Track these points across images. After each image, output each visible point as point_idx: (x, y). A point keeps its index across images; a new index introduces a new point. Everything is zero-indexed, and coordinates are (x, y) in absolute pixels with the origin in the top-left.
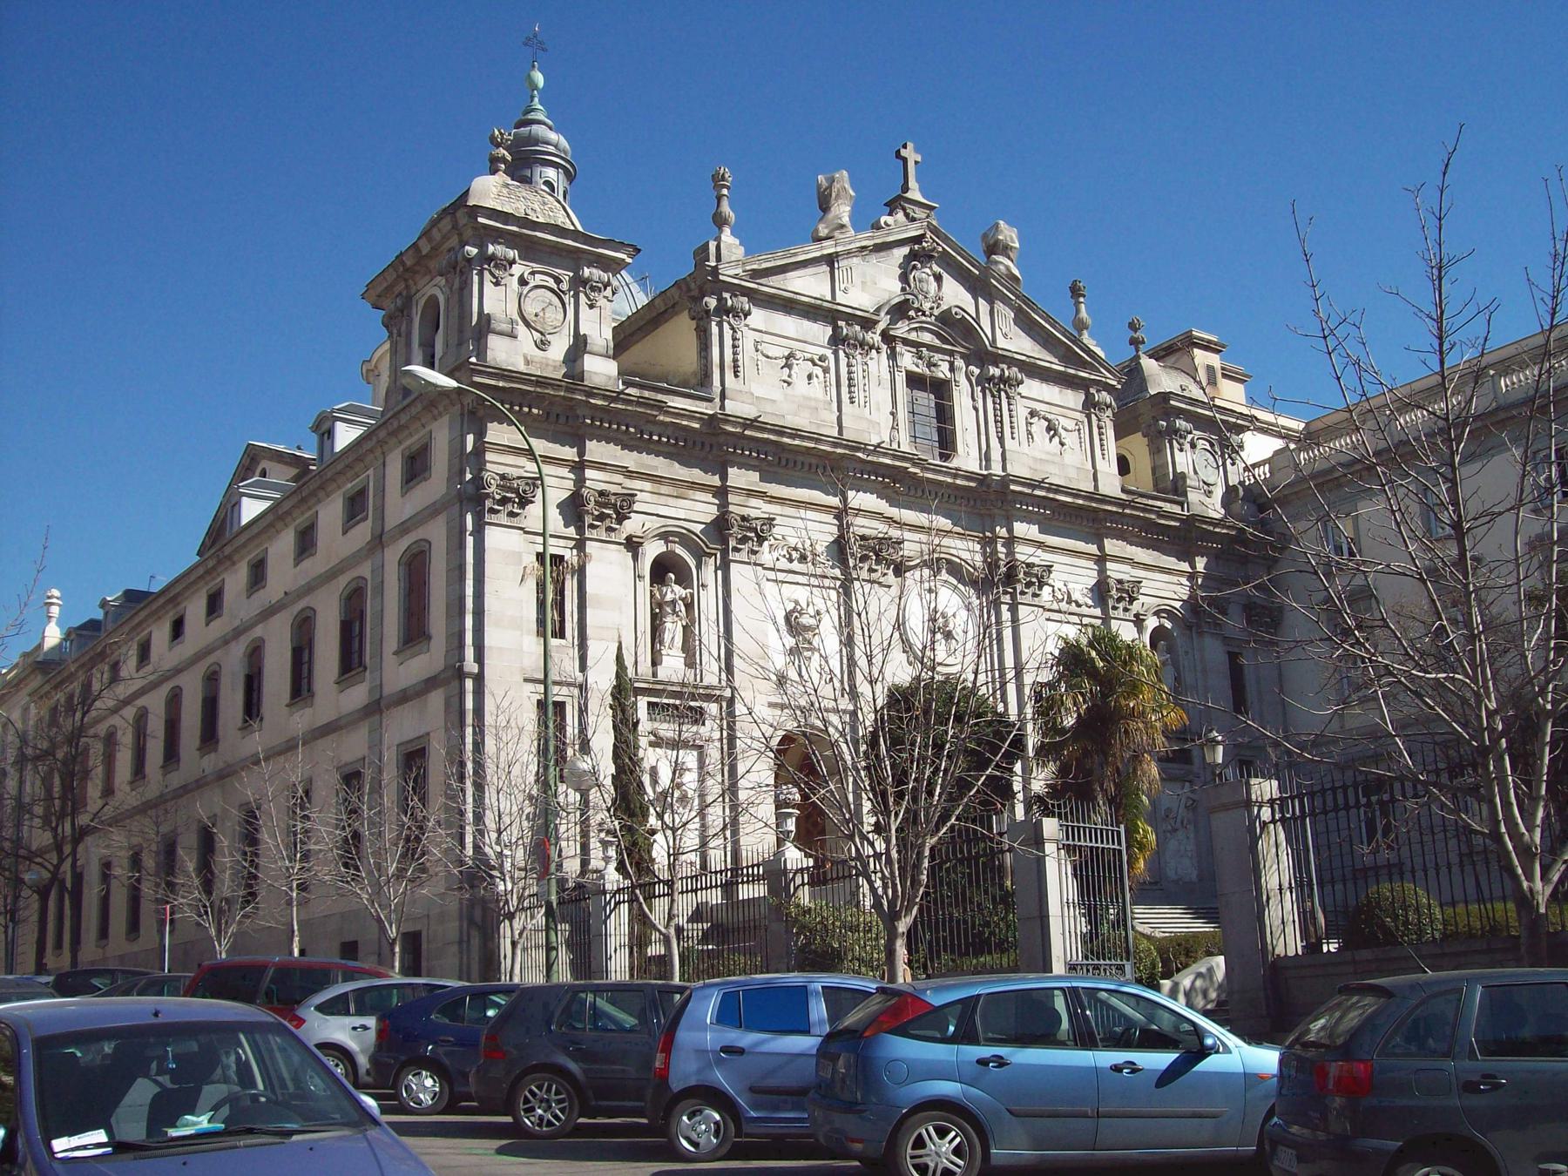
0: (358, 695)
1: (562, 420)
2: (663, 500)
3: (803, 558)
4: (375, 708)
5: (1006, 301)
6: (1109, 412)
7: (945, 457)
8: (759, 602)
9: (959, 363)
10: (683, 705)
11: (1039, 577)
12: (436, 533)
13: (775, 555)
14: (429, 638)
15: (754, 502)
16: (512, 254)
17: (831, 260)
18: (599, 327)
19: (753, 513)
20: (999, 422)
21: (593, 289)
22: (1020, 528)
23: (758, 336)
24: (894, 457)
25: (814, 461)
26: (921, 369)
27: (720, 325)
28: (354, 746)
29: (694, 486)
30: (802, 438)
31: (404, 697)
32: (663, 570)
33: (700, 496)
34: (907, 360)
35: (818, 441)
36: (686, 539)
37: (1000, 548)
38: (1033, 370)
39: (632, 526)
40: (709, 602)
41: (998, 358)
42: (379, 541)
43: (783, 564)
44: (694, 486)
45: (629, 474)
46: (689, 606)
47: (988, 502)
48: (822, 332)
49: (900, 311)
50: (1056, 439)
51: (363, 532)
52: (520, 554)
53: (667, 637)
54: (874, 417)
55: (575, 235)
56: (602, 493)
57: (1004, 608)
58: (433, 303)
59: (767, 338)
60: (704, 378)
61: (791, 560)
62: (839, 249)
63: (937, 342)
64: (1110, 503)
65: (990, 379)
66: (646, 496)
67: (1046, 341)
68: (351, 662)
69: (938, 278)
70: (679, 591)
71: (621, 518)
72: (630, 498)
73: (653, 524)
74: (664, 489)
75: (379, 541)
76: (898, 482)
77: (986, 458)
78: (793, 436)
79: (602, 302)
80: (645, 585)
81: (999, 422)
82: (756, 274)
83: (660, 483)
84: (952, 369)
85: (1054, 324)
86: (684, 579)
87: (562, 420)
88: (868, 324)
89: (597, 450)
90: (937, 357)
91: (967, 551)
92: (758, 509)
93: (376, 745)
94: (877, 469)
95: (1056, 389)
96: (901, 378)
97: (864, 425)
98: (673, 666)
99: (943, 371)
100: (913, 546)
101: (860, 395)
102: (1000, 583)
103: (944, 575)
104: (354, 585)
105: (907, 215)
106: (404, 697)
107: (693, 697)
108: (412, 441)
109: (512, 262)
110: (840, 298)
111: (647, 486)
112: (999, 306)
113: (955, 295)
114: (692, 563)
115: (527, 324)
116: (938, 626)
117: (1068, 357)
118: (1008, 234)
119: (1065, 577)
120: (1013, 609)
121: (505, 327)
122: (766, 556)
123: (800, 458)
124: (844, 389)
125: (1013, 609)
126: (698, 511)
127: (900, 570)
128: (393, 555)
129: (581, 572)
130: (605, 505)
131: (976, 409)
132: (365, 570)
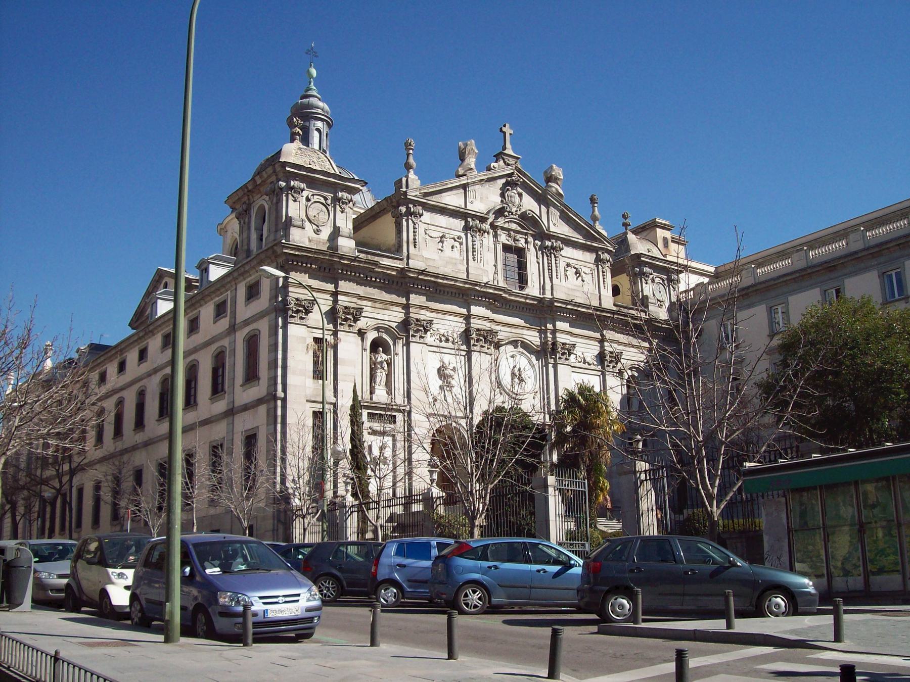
0: (221, 406)
1: (327, 270)
2: (377, 310)
3: (447, 340)
4: (231, 413)
5: (555, 207)
6: (608, 264)
7: (522, 288)
9: (530, 239)
10: (385, 414)
11: (569, 350)
12: (263, 326)
13: (433, 338)
14: (259, 379)
15: (423, 312)
16: (303, 185)
17: (464, 187)
18: (345, 223)
19: (422, 318)
20: (550, 270)
21: (343, 203)
22: (560, 325)
23: (426, 226)
24: (495, 289)
25: (454, 291)
27: (407, 221)
28: (219, 431)
29: (393, 303)
30: (447, 279)
31: (246, 408)
32: (376, 345)
34: (503, 238)
35: (456, 281)
36: (387, 330)
37: (549, 335)
39: (361, 324)
40: (399, 363)
41: (550, 237)
42: (233, 329)
43: (437, 343)
44: (393, 303)
45: (360, 297)
46: (389, 364)
47: (542, 312)
48: (459, 224)
49: (500, 213)
51: (224, 323)
52: (305, 339)
53: (378, 379)
55: (334, 176)
56: (346, 308)
57: (550, 366)
58: (262, 208)
60: (398, 248)
61: (441, 341)
63: (519, 229)
65: (546, 247)
66: (368, 310)
68: (217, 389)
69: (520, 195)
70: (385, 357)
71: (356, 320)
72: (360, 310)
73: (371, 323)
74: (378, 305)
75: (233, 329)
76: (497, 301)
77: (543, 288)
78: (443, 279)
79: (347, 209)
80: (367, 354)
81: (550, 270)
84: (526, 242)
86: (387, 351)
87: (327, 270)
88: (483, 220)
89: (344, 286)
90: (518, 236)
91: (533, 337)
92: (424, 315)
93: (231, 431)
94: (486, 295)
95: (581, 252)
96: (500, 247)
97: (480, 272)
98: (381, 395)
99: (522, 243)
100: (504, 334)
102: (548, 352)
104: (219, 350)
105: (505, 162)
106: (246, 408)
107: (389, 410)
108: (251, 279)
110: (469, 207)
111: (369, 303)
112: (552, 209)
113: (529, 204)
114: (391, 342)
115: (310, 221)
116: (517, 375)
117: (588, 235)
118: (558, 172)
119: (583, 350)
121: (299, 223)
124: (470, 254)
126: (395, 316)
127: (498, 346)
128: (241, 336)
129: (335, 347)
130: (348, 314)
131: (538, 263)
132: (225, 342)
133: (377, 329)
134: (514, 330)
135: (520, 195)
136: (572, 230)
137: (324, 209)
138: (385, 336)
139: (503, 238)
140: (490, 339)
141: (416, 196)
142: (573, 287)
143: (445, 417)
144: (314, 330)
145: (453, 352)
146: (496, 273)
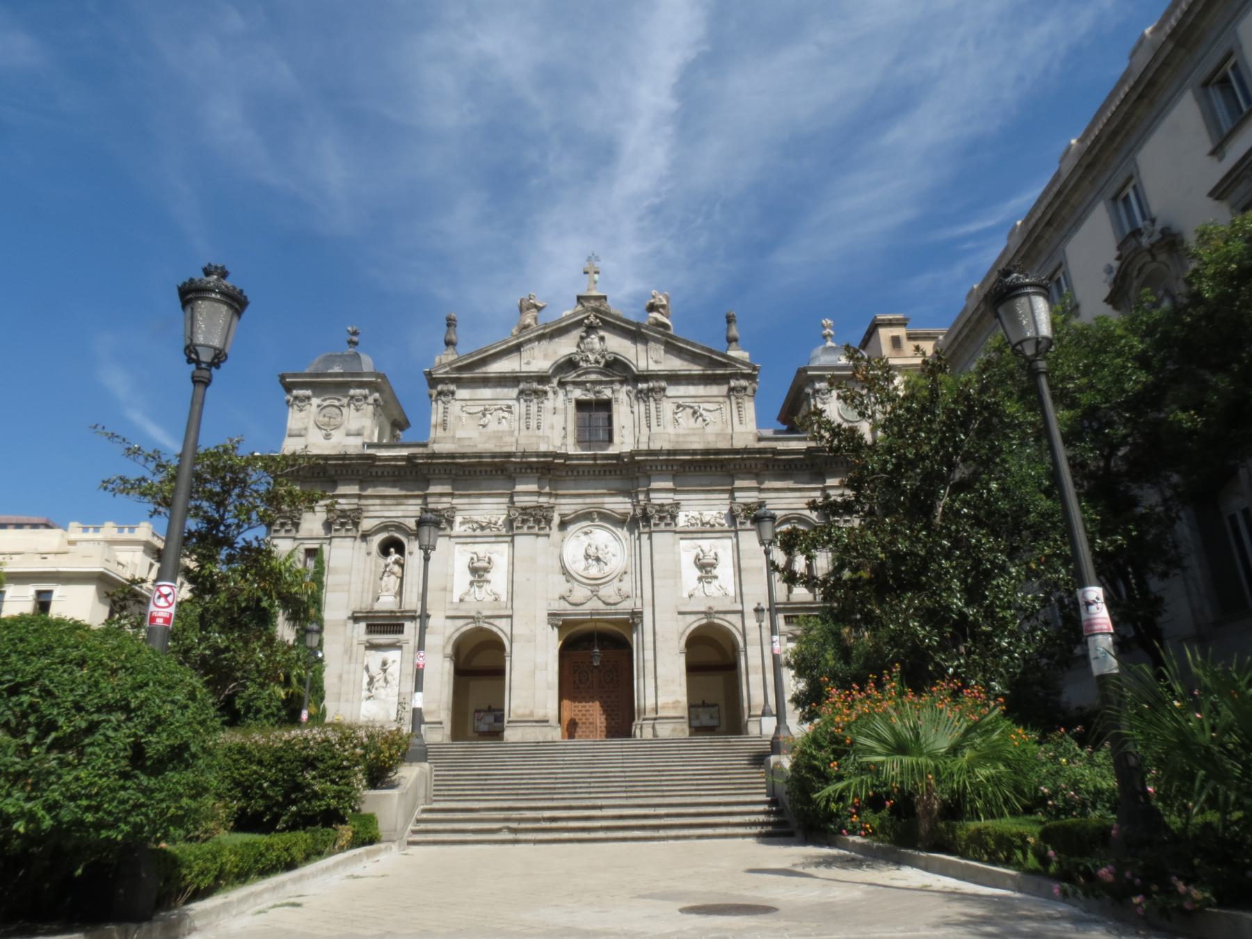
5: (656, 340)
8: (453, 558)
9: (617, 386)
11: (668, 515)
15: (444, 499)
16: (308, 392)
19: (440, 507)
20: (648, 417)
21: (358, 400)
23: (463, 403)
25: (489, 469)
26: (591, 396)
33: (412, 501)
38: (675, 378)
39: (366, 524)
41: (646, 377)
43: (470, 532)
50: (700, 419)
54: (548, 432)
55: (342, 375)
67: (693, 357)
69: (602, 339)
71: (356, 524)
73: (376, 522)
74: (387, 502)
81: (648, 417)
82: (460, 369)
85: (693, 345)
88: (543, 379)
90: (598, 388)
91: (620, 505)
92: (443, 504)
94: (530, 466)
99: (607, 393)
101: (533, 424)
103: (597, 522)
109: (309, 398)
111: (378, 501)
112: (652, 344)
120: (650, 538)
122: (458, 529)
123: (478, 469)
124: (523, 421)
125: (650, 538)
126: (408, 512)
133: (384, 528)
134: (588, 500)
135: (602, 339)
136: (685, 363)
137: (337, 411)
138: (397, 535)
139: (578, 393)
140: (536, 519)
141: (446, 373)
143: (472, 617)
145: (493, 539)
146: (565, 437)
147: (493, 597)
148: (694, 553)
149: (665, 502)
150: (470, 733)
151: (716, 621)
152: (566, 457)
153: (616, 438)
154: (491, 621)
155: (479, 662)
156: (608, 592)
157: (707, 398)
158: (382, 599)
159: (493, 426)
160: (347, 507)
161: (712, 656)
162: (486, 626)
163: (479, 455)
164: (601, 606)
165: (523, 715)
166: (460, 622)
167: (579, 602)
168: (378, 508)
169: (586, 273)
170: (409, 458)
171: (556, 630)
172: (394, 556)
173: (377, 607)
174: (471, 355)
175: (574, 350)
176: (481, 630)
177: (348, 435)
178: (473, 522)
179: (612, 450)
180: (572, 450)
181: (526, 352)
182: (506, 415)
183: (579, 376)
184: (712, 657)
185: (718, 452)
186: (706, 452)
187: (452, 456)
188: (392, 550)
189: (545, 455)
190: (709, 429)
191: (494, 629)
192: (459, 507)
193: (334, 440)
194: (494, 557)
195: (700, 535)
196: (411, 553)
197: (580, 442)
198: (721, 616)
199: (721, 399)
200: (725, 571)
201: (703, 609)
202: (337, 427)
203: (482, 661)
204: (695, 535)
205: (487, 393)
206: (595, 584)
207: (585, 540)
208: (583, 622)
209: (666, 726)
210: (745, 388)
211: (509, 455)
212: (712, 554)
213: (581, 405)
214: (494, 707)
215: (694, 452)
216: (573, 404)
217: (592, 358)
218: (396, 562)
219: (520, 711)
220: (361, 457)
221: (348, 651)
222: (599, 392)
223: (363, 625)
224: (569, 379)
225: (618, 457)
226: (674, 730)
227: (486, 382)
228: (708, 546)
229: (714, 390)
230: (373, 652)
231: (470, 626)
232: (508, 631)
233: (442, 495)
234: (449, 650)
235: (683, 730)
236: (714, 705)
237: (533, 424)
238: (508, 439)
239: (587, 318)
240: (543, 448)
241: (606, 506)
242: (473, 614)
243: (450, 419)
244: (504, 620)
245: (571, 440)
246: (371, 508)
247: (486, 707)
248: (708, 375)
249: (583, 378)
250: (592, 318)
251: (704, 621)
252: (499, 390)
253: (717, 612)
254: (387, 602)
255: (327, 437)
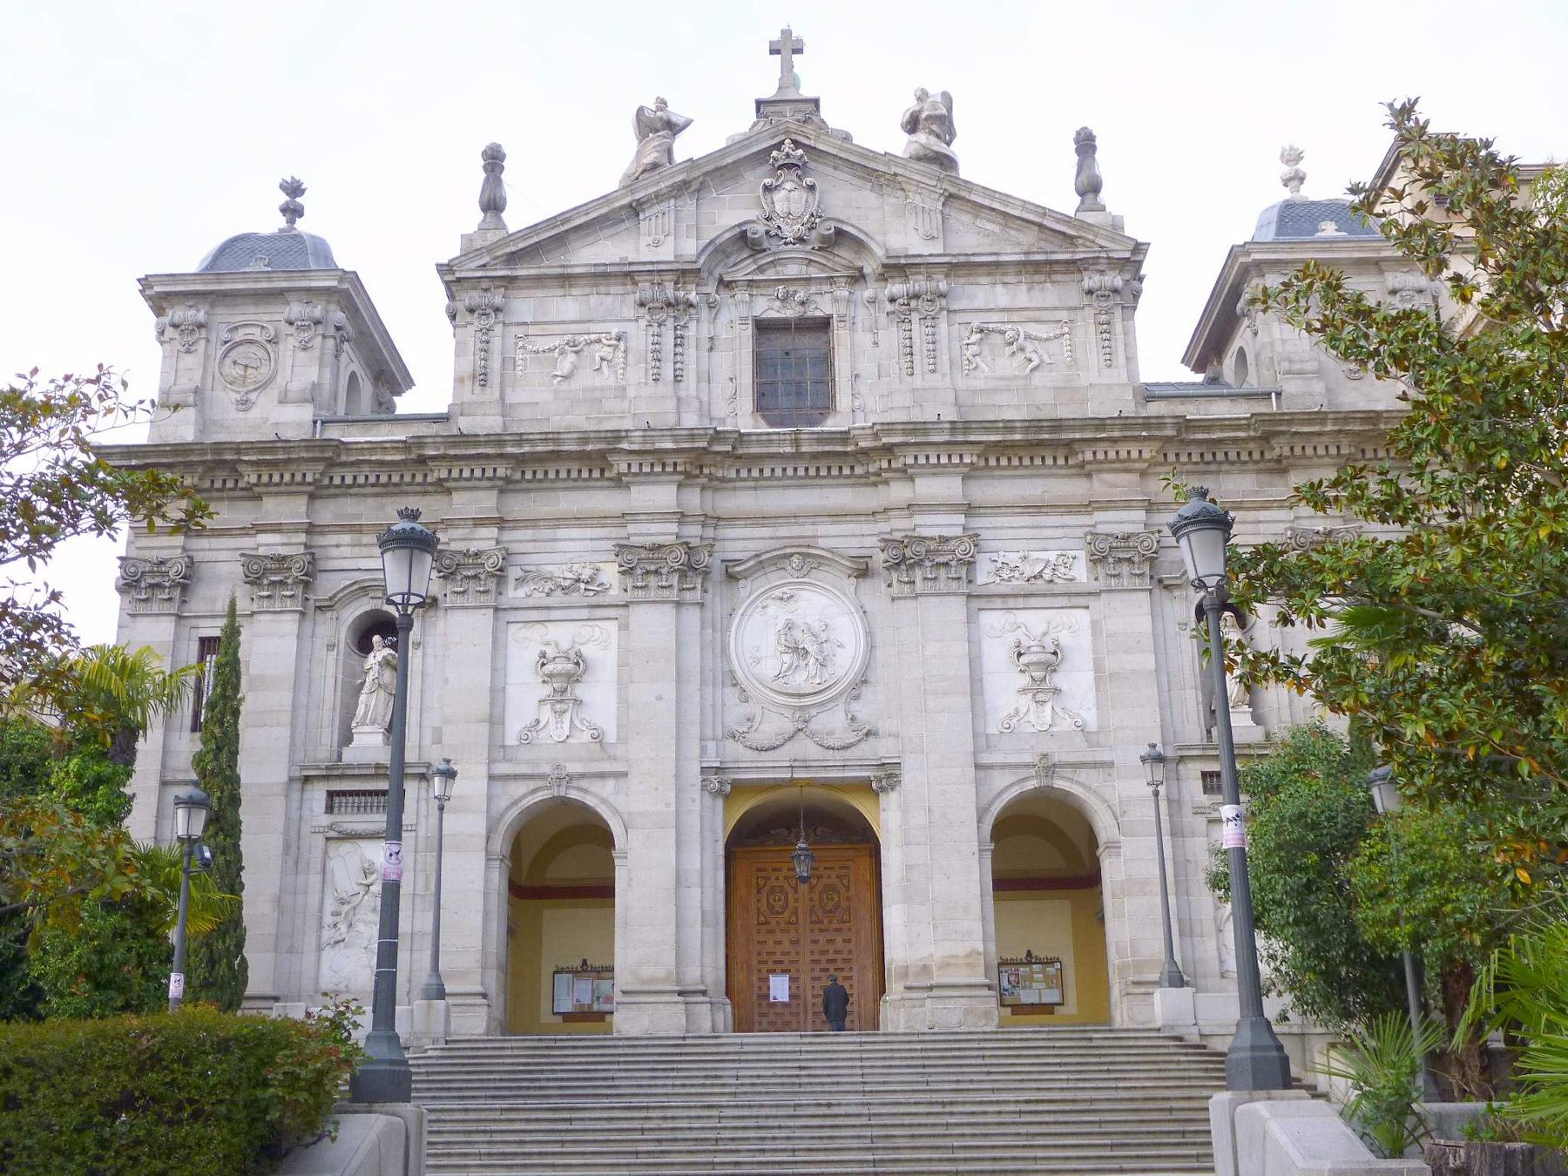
13: (521, 593)
15: (484, 532)
19: (474, 547)
23: (520, 331)
39: (327, 586)
59: (532, 330)
62: (637, 196)
64: (1073, 429)
73: (344, 580)
82: (513, 258)
83: (361, 532)
88: (684, 274)
92: (484, 540)
99: (823, 306)
111: (346, 538)
134: (783, 531)
137: (261, 353)
142: (992, 384)
143: (542, 777)
144: (201, 623)
145: (585, 613)
147: (586, 737)
148: (1011, 639)
149: (947, 532)
150: (546, 1018)
151: (1059, 784)
152: (741, 438)
153: (843, 400)
154: (584, 784)
155: (558, 865)
156: (833, 722)
157: (1035, 315)
158: (358, 740)
159: (585, 379)
160: (283, 551)
161: (1044, 854)
162: (574, 794)
163: (555, 437)
164: (811, 750)
165: (652, 980)
166: (519, 789)
167: (766, 744)
168: (347, 551)
169: (774, 51)
170: (406, 446)
171: (720, 802)
172: (381, 651)
173: (349, 755)
174: (534, 229)
175: (752, 214)
176: (563, 804)
177: (283, 401)
178: (546, 579)
179: (831, 425)
180: (746, 421)
181: (650, 222)
182: (606, 352)
183: (761, 269)
184: (1047, 860)
185: (1057, 425)
186: (1034, 425)
187: (497, 440)
188: (376, 639)
189: (692, 435)
190: (1037, 380)
191: (590, 801)
192: (514, 548)
193: (254, 414)
194: (585, 651)
195: (1021, 602)
196: (417, 645)
197: (764, 403)
198: (1068, 772)
199: (1064, 315)
200: (1077, 681)
201: (1027, 758)
202: (263, 387)
203: (565, 870)
204: (1011, 603)
205: (567, 306)
206: (803, 707)
207: (777, 614)
208: (777, 784)
209: (951, 1004)
210: (1116, 291)
211: (617, 436)
212: (1048, 642)
213: (763, 328)
214: (594, 962)
215: (1008, 426)
216: (749, 330)
217: (790, 231)
218: (386, 663)
219: (647, 972)
220: (309, 444)
221: (292, 849)
222: (803, 303)
223: (317, 795)
224: (739, 276)
225: (844, 437)
226: (968, 1012)
227: (566, 280)
228: (1036, 622)
229: (1050, 294)
230: (346, 847)
231: (539, 796)
232: (620, 802)
233: (479, 522)
234: (500, 844)
235: (987, 1013)
236: (1051, 962)
237: (668, 372)
238: (612, 405)
239: (778, 147)
240: (690, 421)
241: (822, 542)
242: (546, 769)
243: (495, 363)
244: (611, 783)
245: (747, 402)
246: (334, 552)
247: (577, 963)
248: (1037, 263)
249: (770, 274)
250: (787, 146)
251: (1031, 785)
252: (594, 299)
253: (1063, 765)
254: (369, 744)
255: (245, 404)
